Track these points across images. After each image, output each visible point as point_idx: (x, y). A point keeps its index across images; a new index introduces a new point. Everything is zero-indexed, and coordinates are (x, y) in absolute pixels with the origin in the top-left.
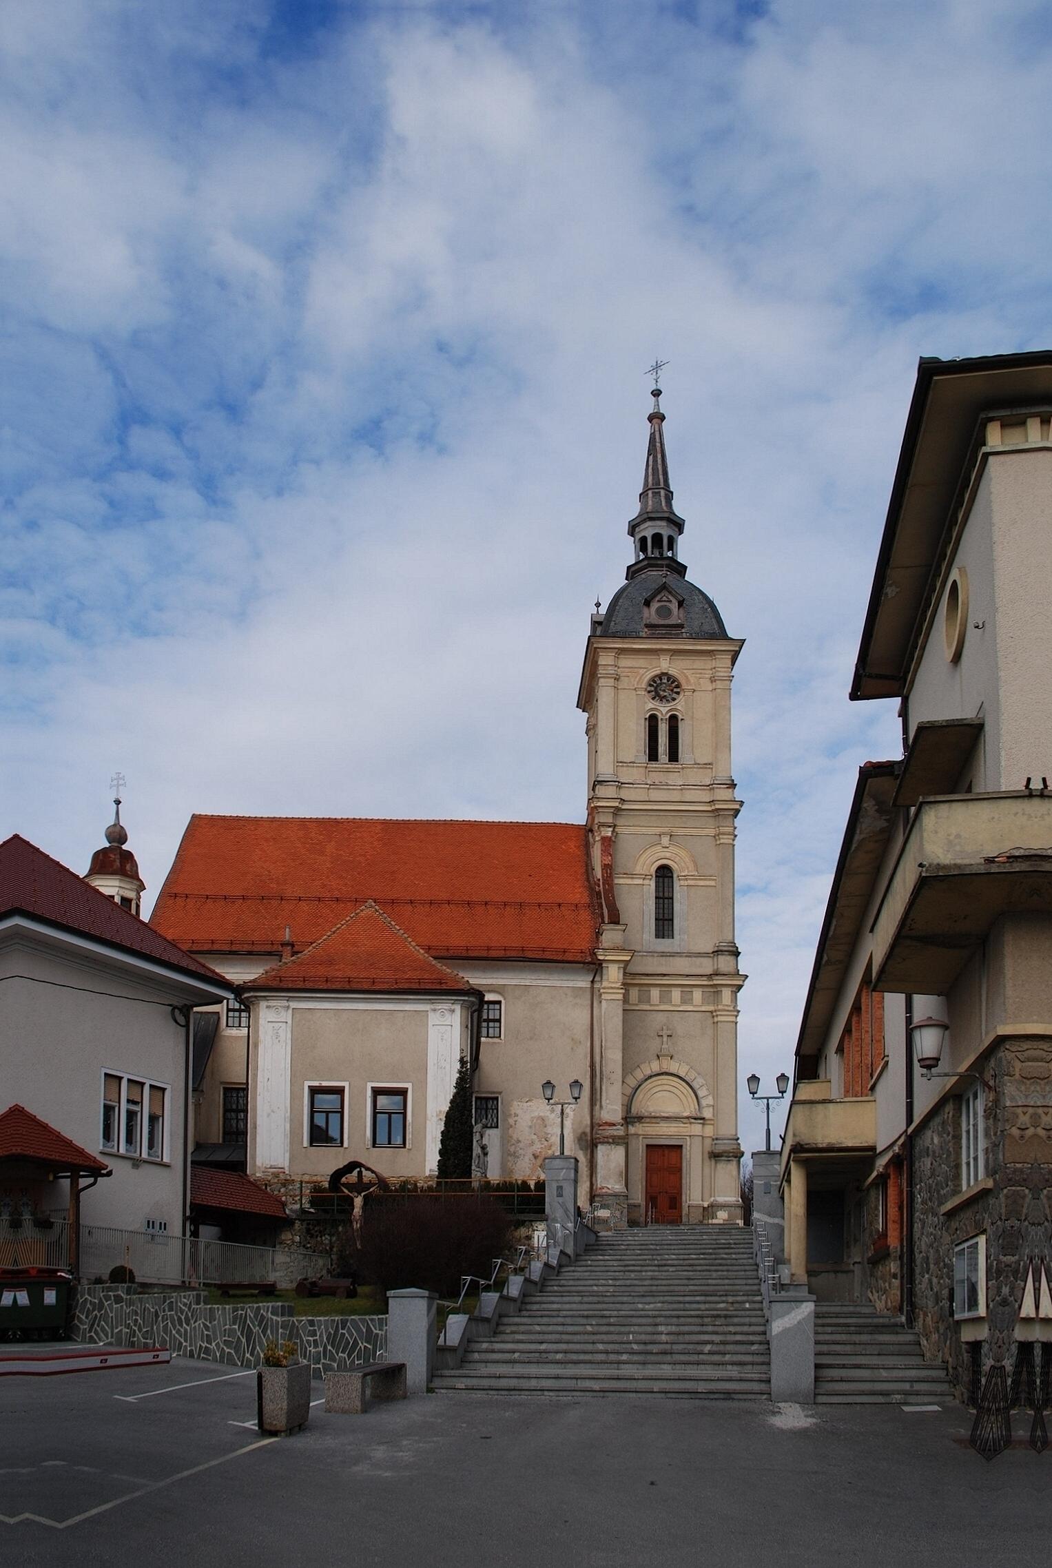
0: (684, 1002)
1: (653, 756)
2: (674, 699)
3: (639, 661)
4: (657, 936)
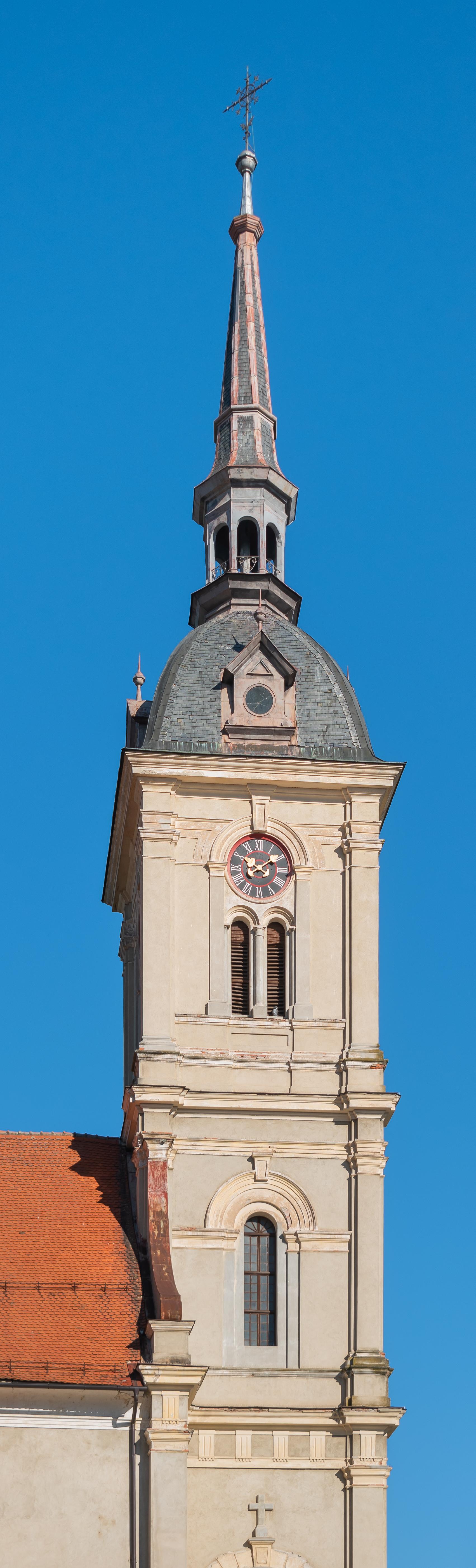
0: (294, 1453)
1: (242, 1004)
2: (277, 889)
3: (217, 806)
4: (248, 1341)
